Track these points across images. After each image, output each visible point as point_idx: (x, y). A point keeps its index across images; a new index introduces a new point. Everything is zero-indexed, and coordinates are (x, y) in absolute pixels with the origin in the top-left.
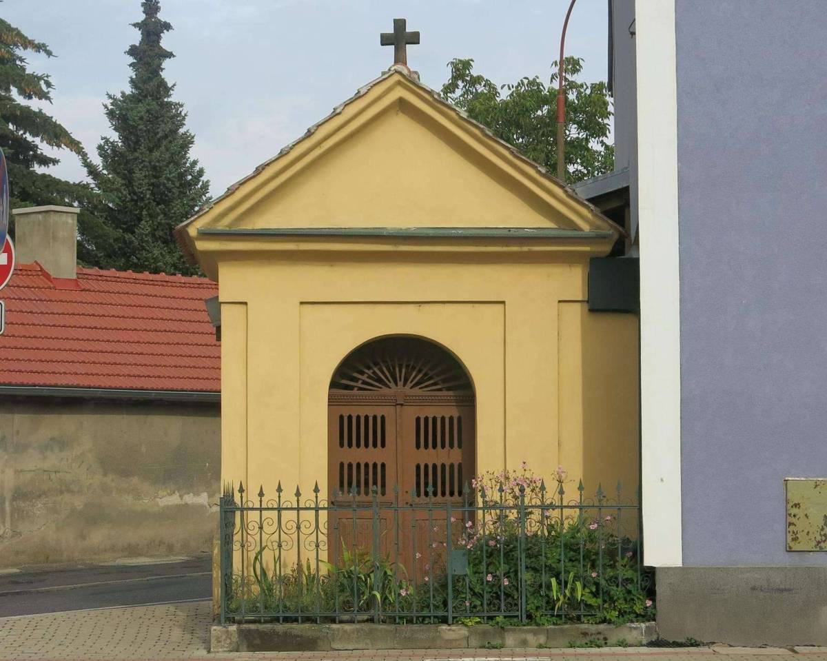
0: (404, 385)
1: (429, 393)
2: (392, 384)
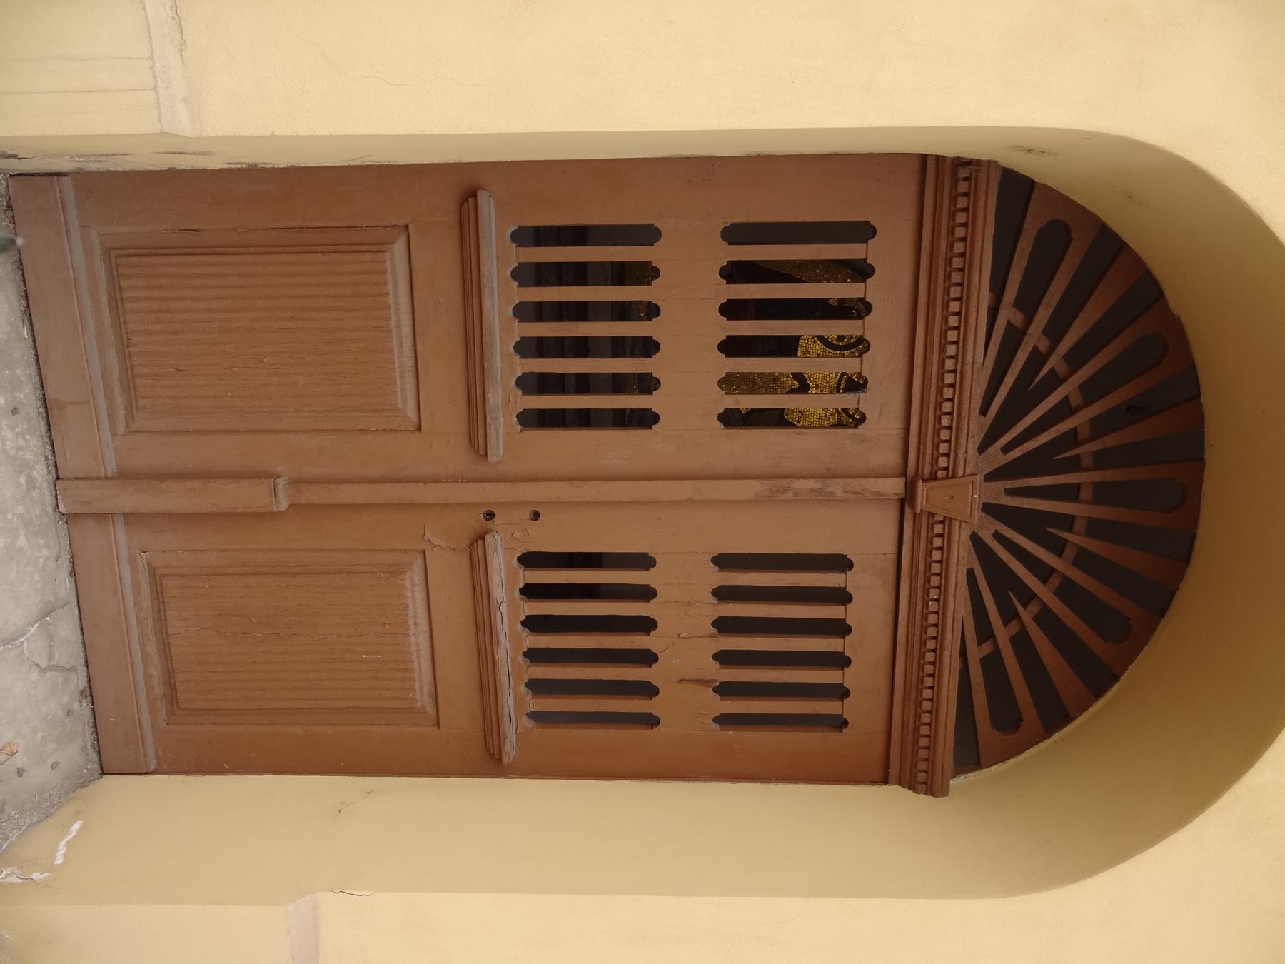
0: (988, 508)
2: (996, 457)
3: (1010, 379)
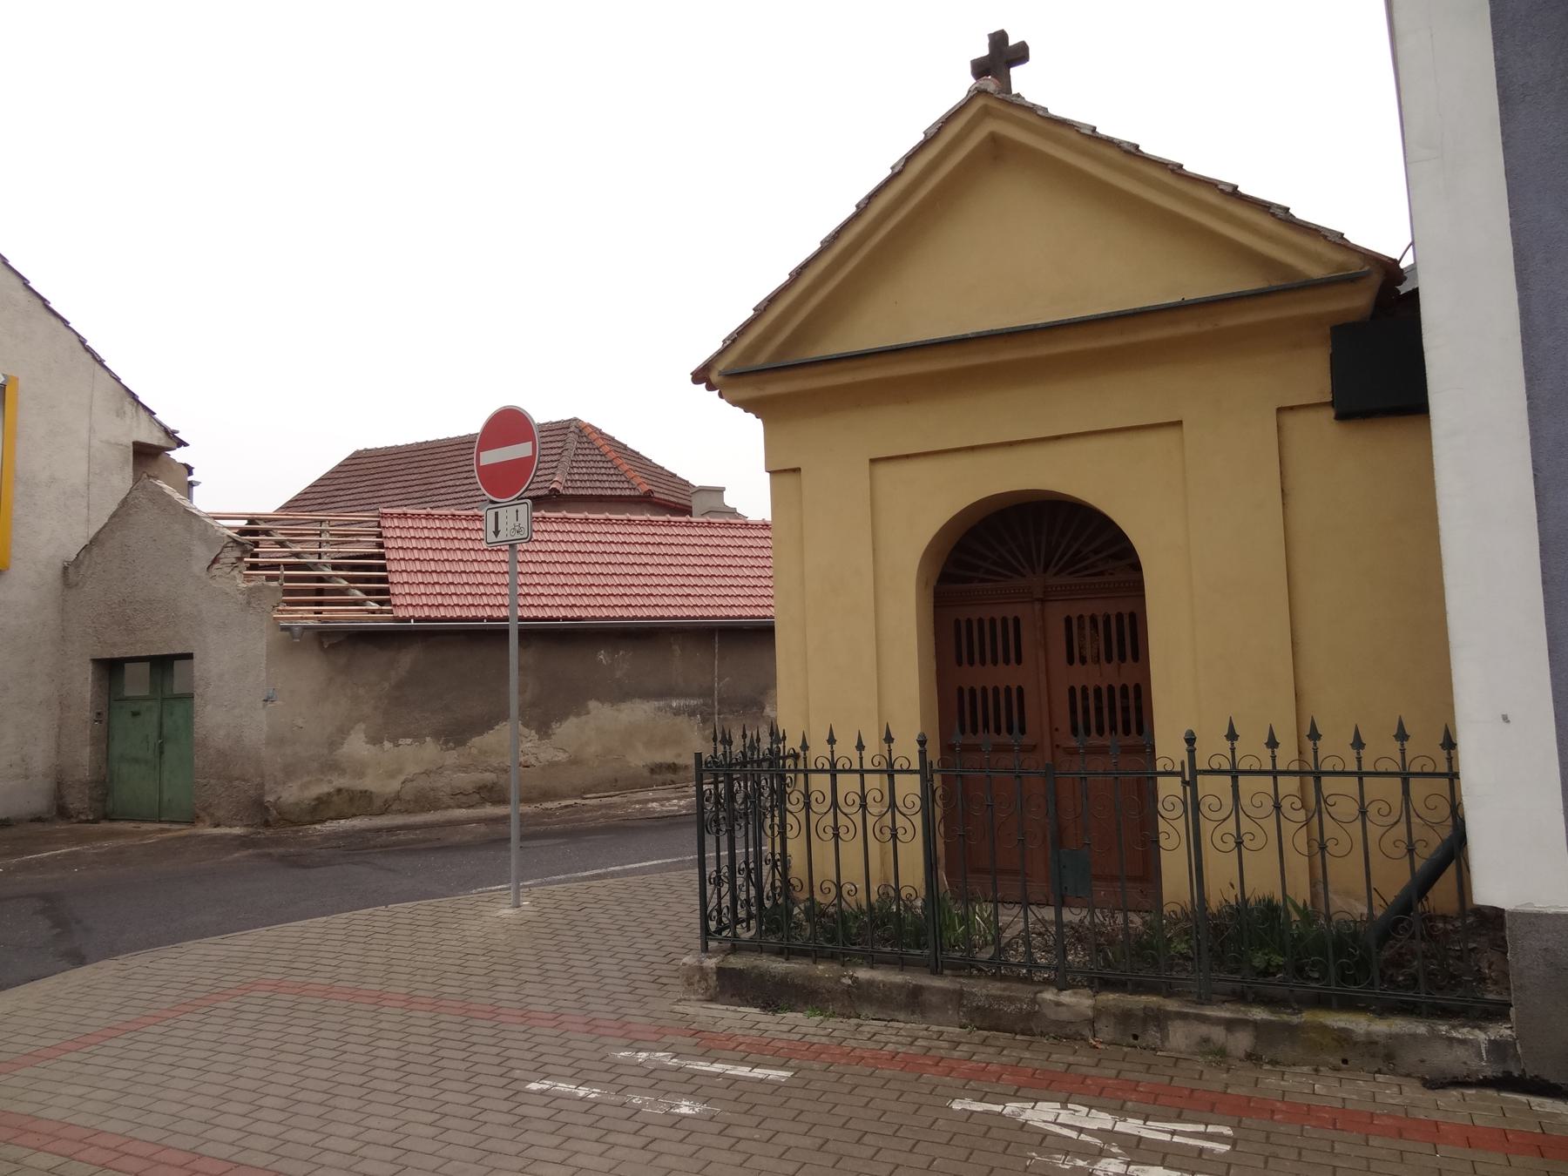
3: (1000, 570)
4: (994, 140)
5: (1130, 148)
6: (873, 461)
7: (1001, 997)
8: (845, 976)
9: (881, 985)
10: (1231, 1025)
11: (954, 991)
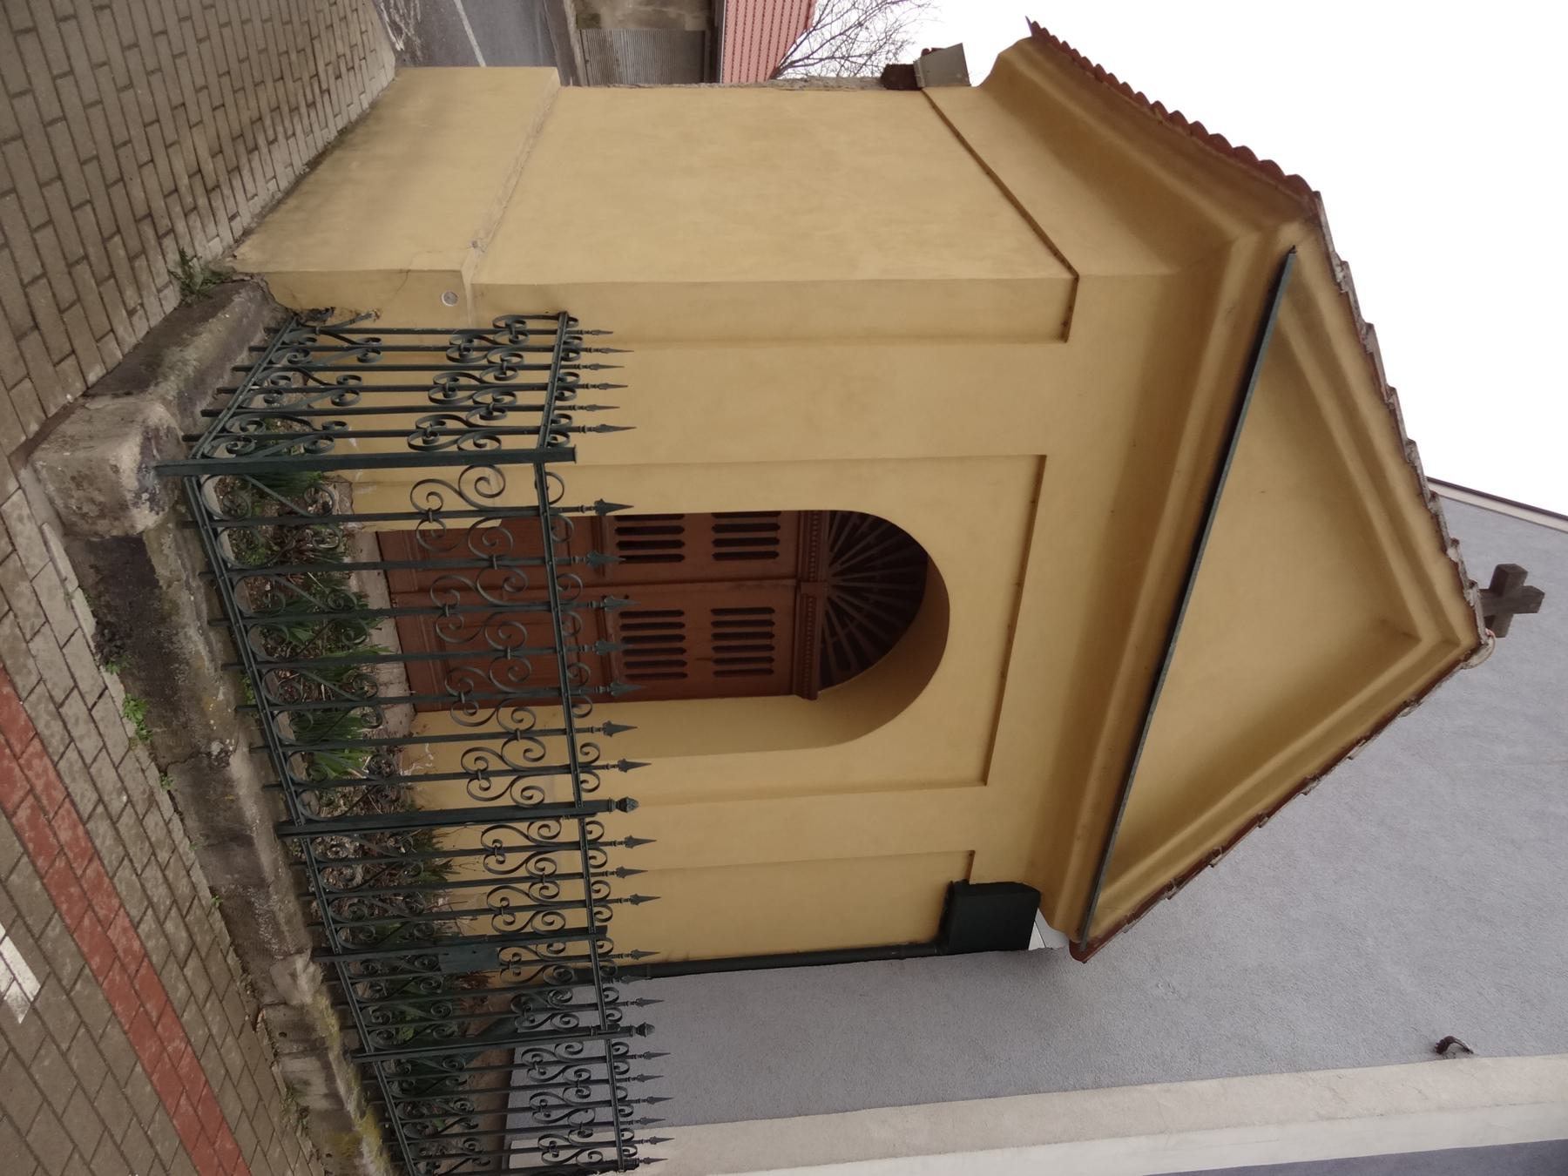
1: (818, 645)
2: (837, 567)
3: (843, 538)
4: (1408, 637)
5: (1307, 789)
6: (1042, 459)
7: (276, 924)
8: (222, 742)
9: (231, 798)
10: (333, 1095)
11: (263, 880)
